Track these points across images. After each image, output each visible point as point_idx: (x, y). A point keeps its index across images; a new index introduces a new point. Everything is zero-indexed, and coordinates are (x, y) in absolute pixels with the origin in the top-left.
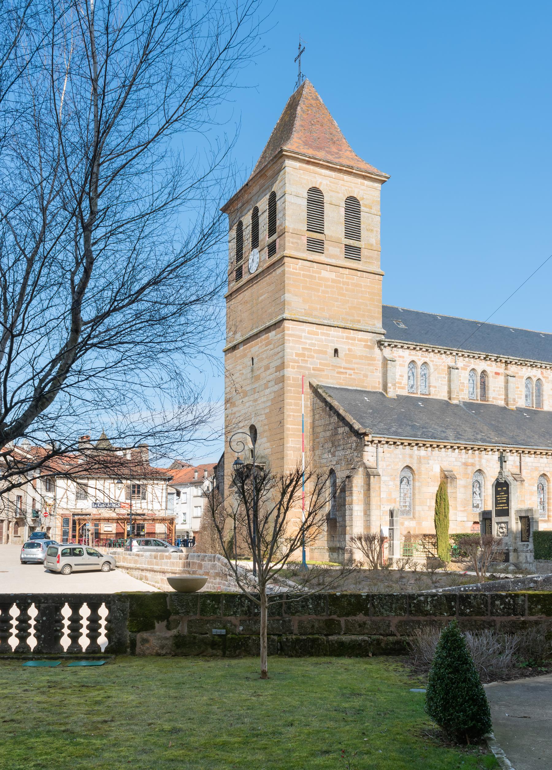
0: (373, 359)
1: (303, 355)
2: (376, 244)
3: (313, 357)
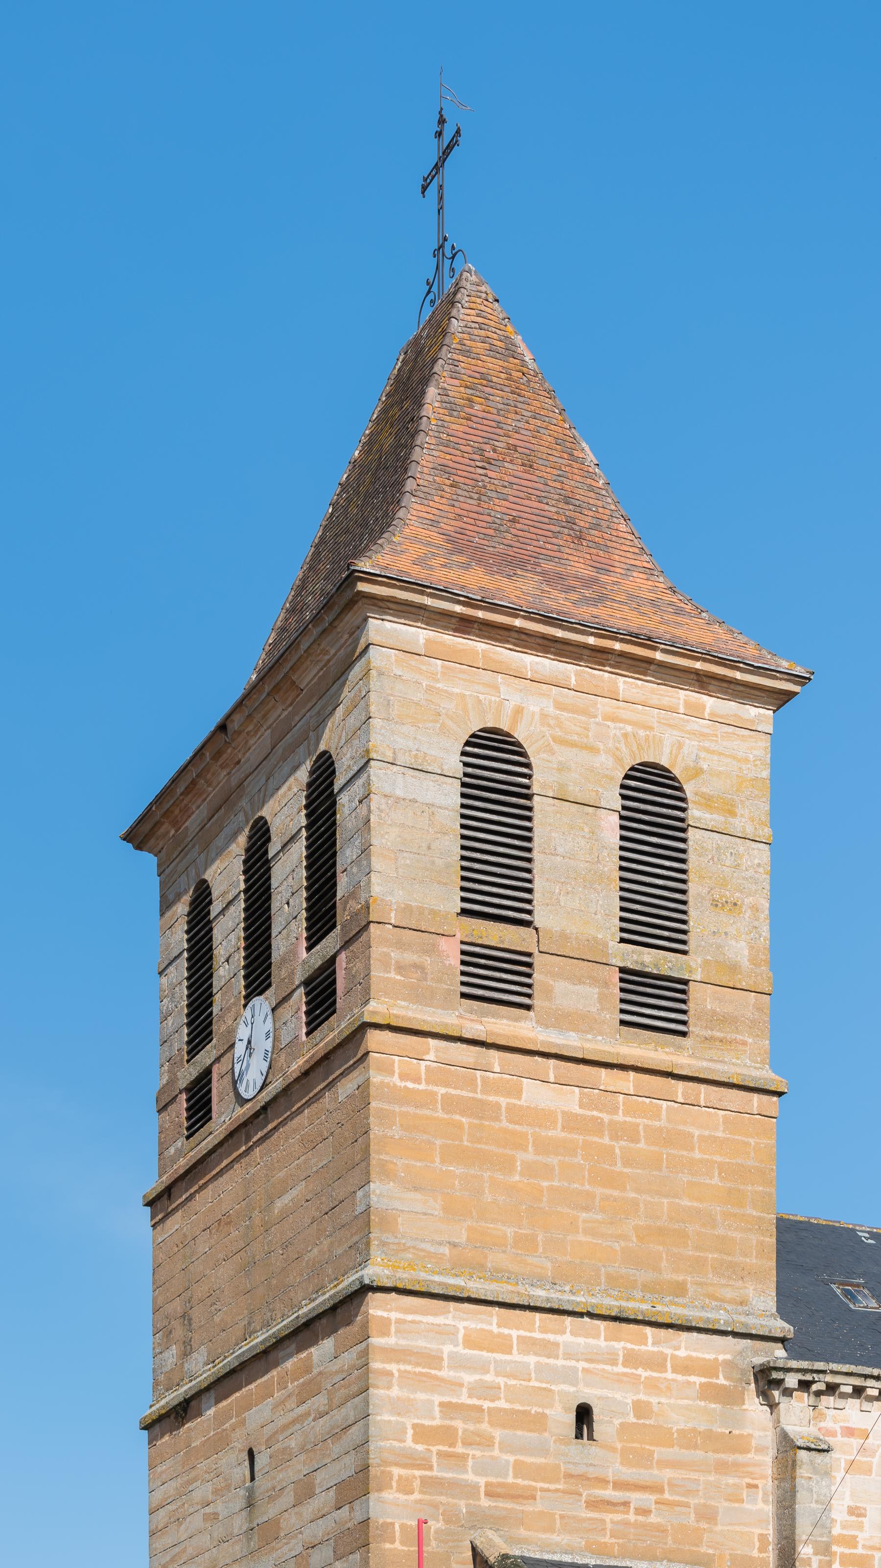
0: (740, 1445)
1: (446, 1435)
2: (753, 960)
3: (486, 1442)
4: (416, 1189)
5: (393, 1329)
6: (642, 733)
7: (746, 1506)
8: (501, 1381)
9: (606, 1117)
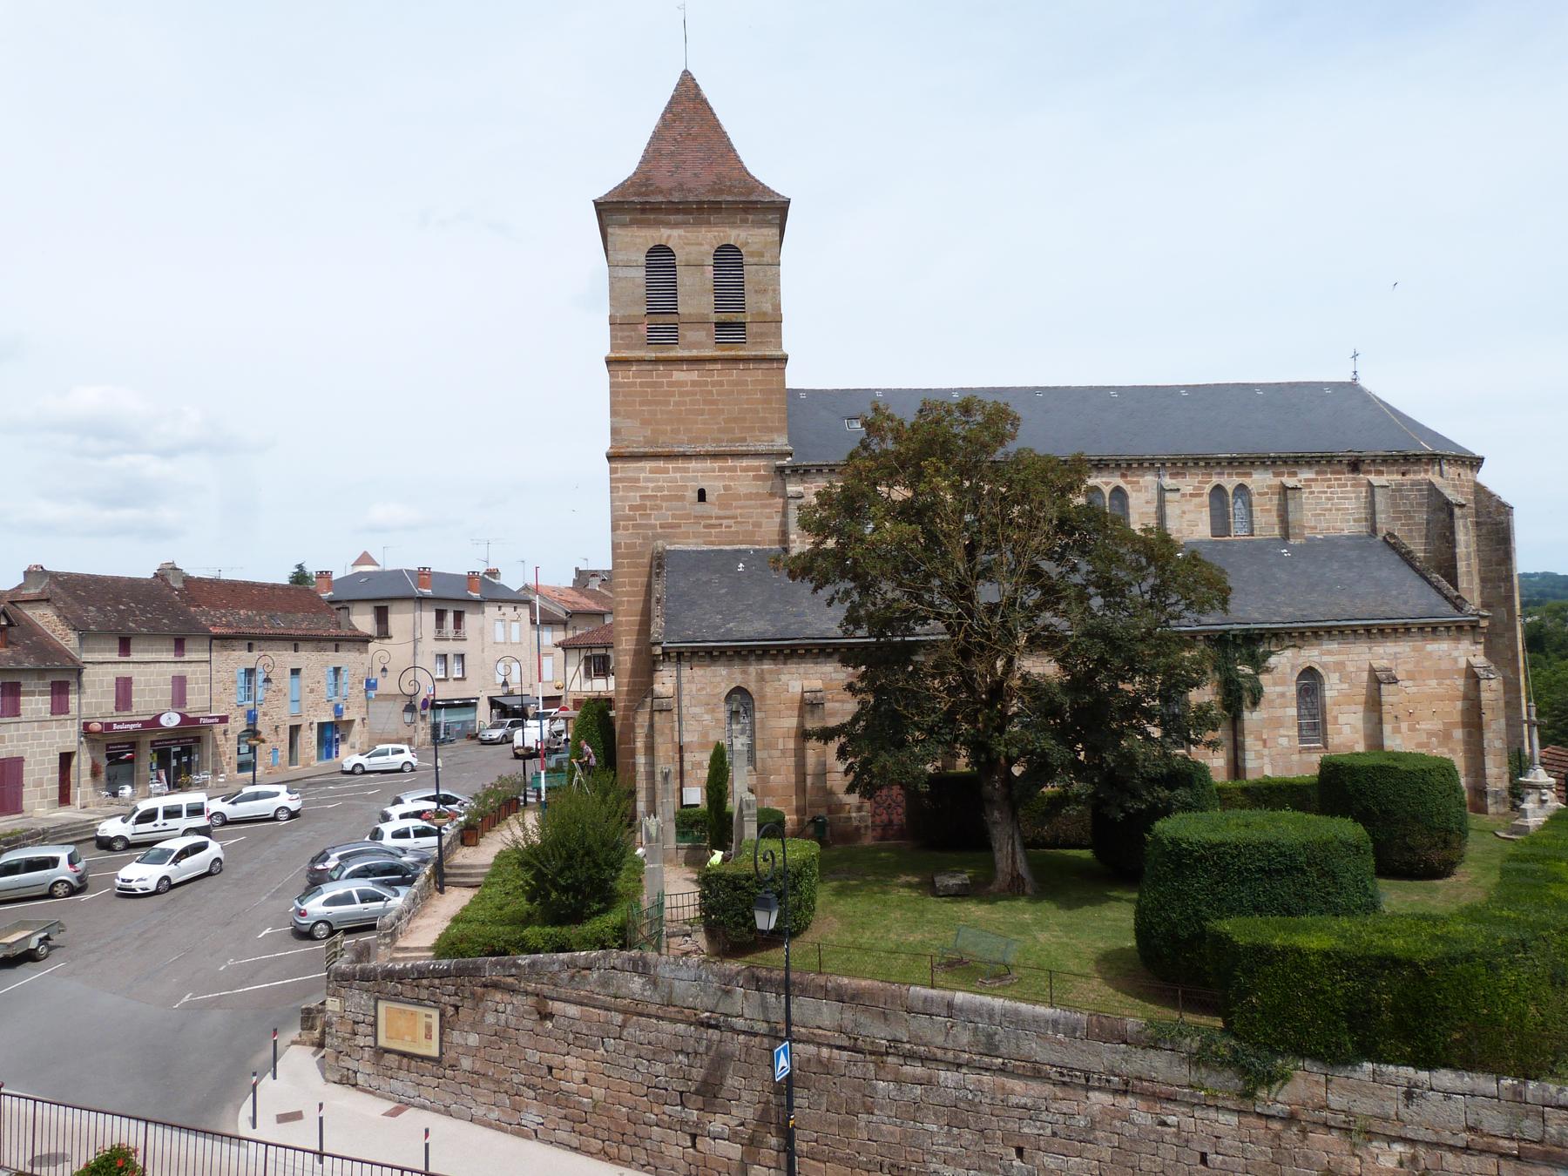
1: (642, 507)
3: (659, 508)
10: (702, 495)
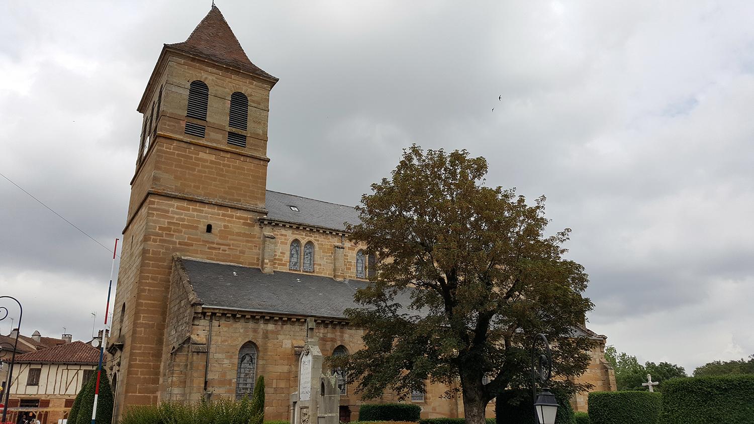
1: (168, 229)
4: (167, 173)
5: (156, 203)
6: (238, 86)
7: (253, 251)
8: (186, 218)
9: (222, 162)
10: (209, 228)
